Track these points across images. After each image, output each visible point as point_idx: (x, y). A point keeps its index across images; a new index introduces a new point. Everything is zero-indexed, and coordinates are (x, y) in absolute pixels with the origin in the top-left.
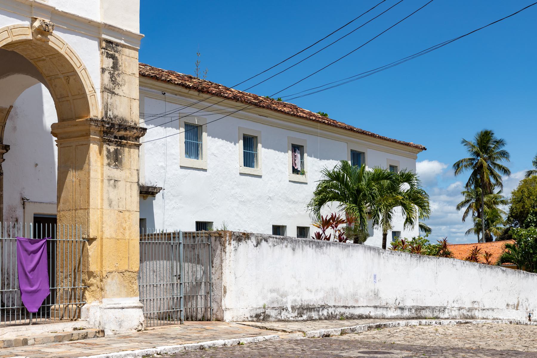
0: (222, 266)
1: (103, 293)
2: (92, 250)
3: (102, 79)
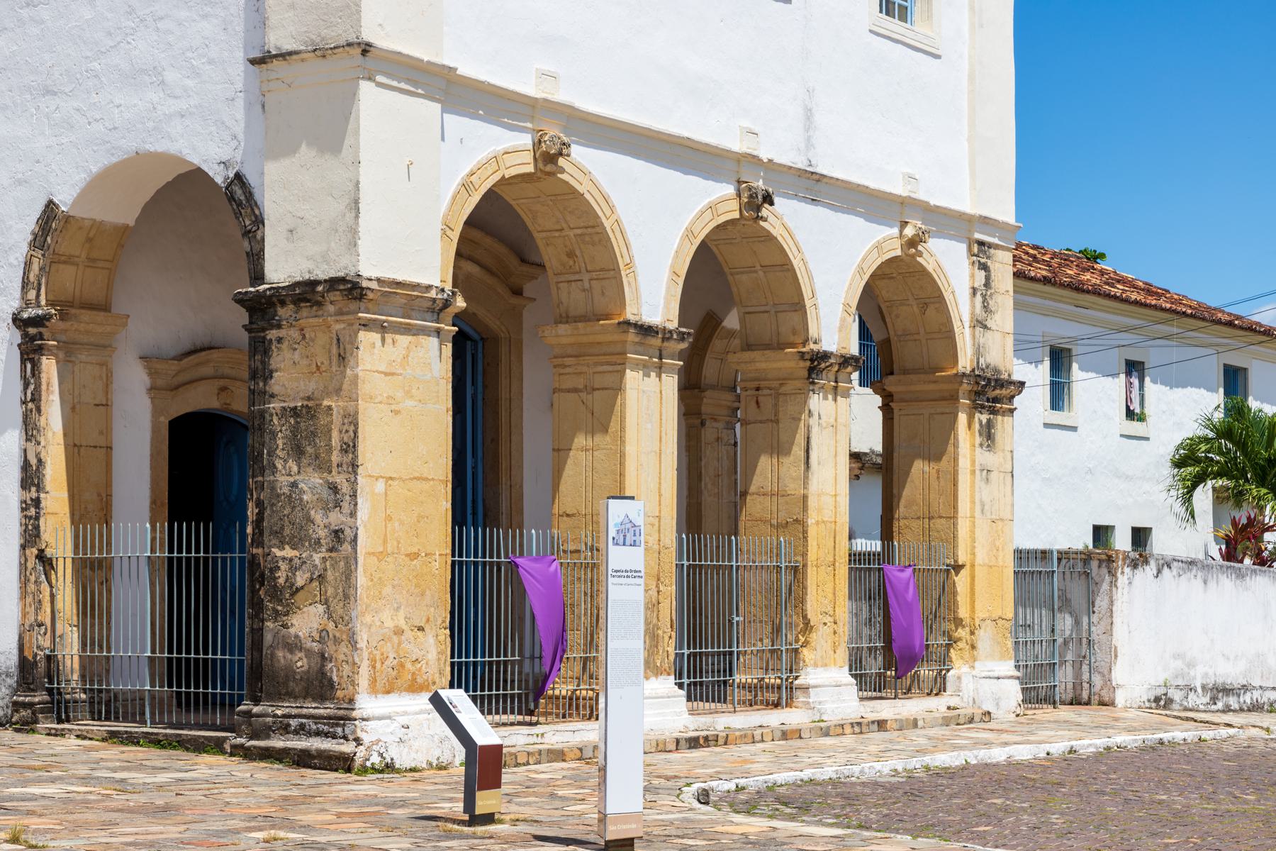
0: (1112, 610)
1: (975, 653)
2: (961, 583)
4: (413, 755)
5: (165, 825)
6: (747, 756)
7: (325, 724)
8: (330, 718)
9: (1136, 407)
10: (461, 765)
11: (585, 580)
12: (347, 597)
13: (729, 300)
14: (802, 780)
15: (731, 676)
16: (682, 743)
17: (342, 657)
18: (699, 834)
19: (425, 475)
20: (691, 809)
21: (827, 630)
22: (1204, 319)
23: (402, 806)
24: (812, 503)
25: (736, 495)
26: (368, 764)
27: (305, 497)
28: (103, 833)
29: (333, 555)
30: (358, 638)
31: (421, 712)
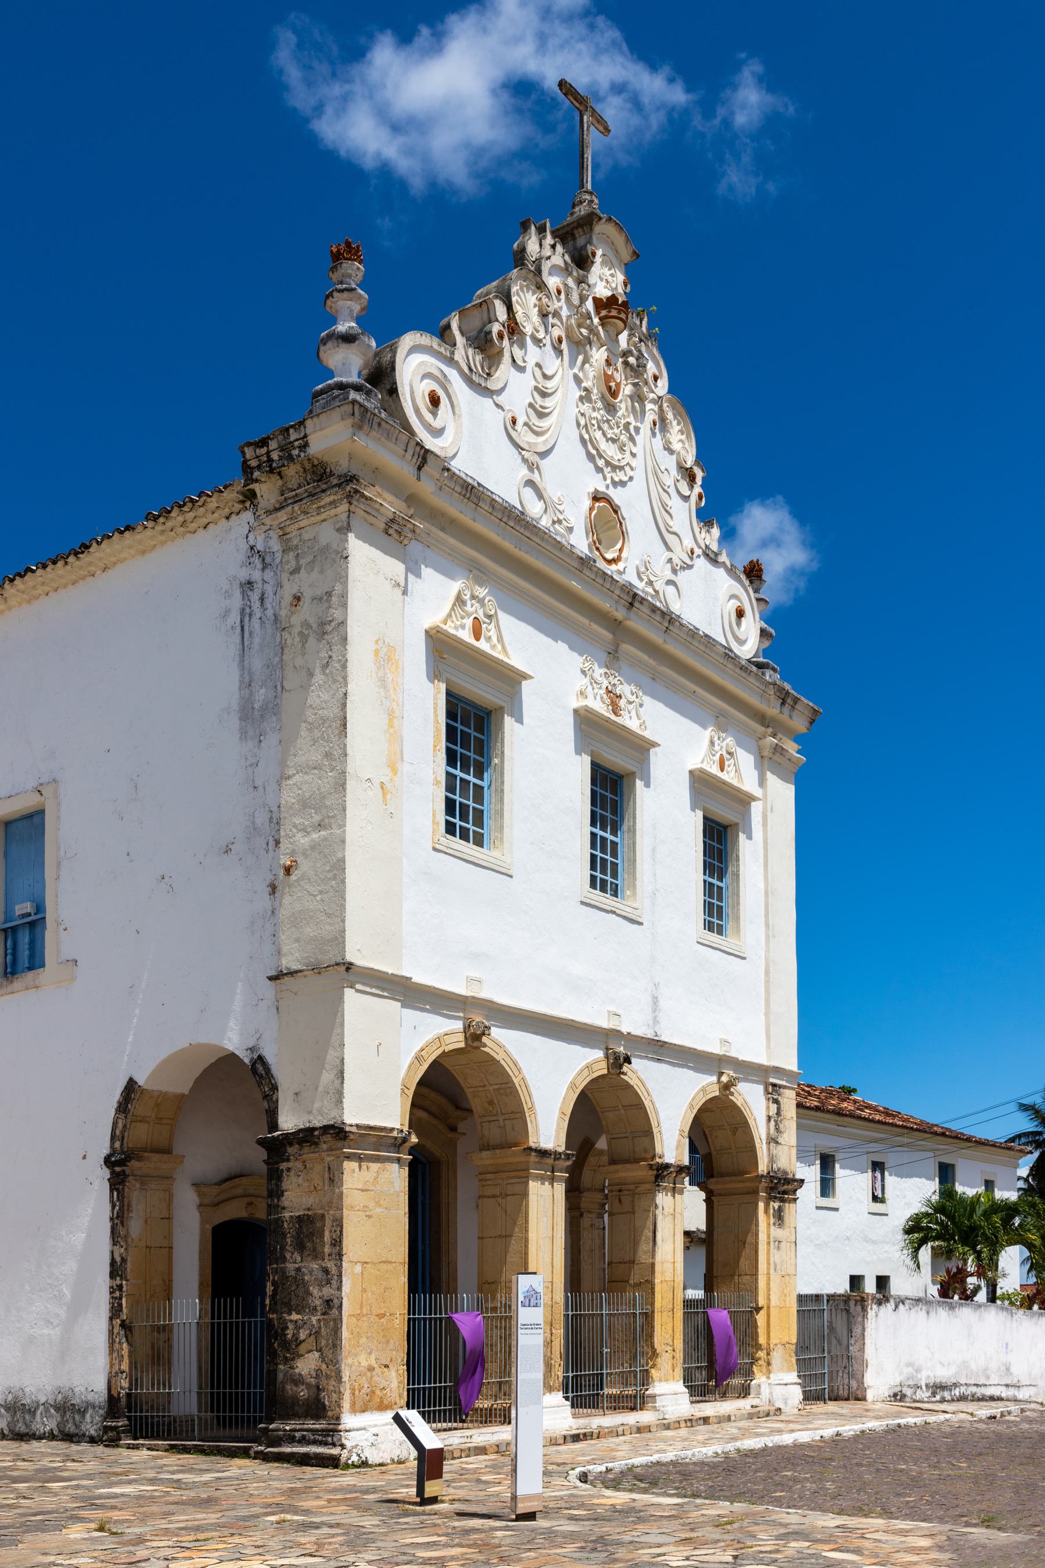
3: (768, 1129)
4: (381, 1454)
5: (207, 1513)
6: (613, 1446)
7: (319, 1435)
8: (323, 1430)
9: (879, 1193)
10: (415, 1460)
11: (501, 1327)
12: (336, 1344)
13: (599, 1130)
14: (652, 1462)
15: (601, 1390)
16: (568, 1438)
17: (331, 1388)
18: (582, 1506)
19: (389, 1260)
20: (575, 1487)
21: (668, 1356)
22: (925, 1132)
23: (373, 1492)
24: (658, 1268)
25: (604, 1263)
26: (350, 1462)
27: (306, 1278)
28: (164, 1521)
29: (325, 1317)
30: (343, 1375)
31: (386, 1424)
